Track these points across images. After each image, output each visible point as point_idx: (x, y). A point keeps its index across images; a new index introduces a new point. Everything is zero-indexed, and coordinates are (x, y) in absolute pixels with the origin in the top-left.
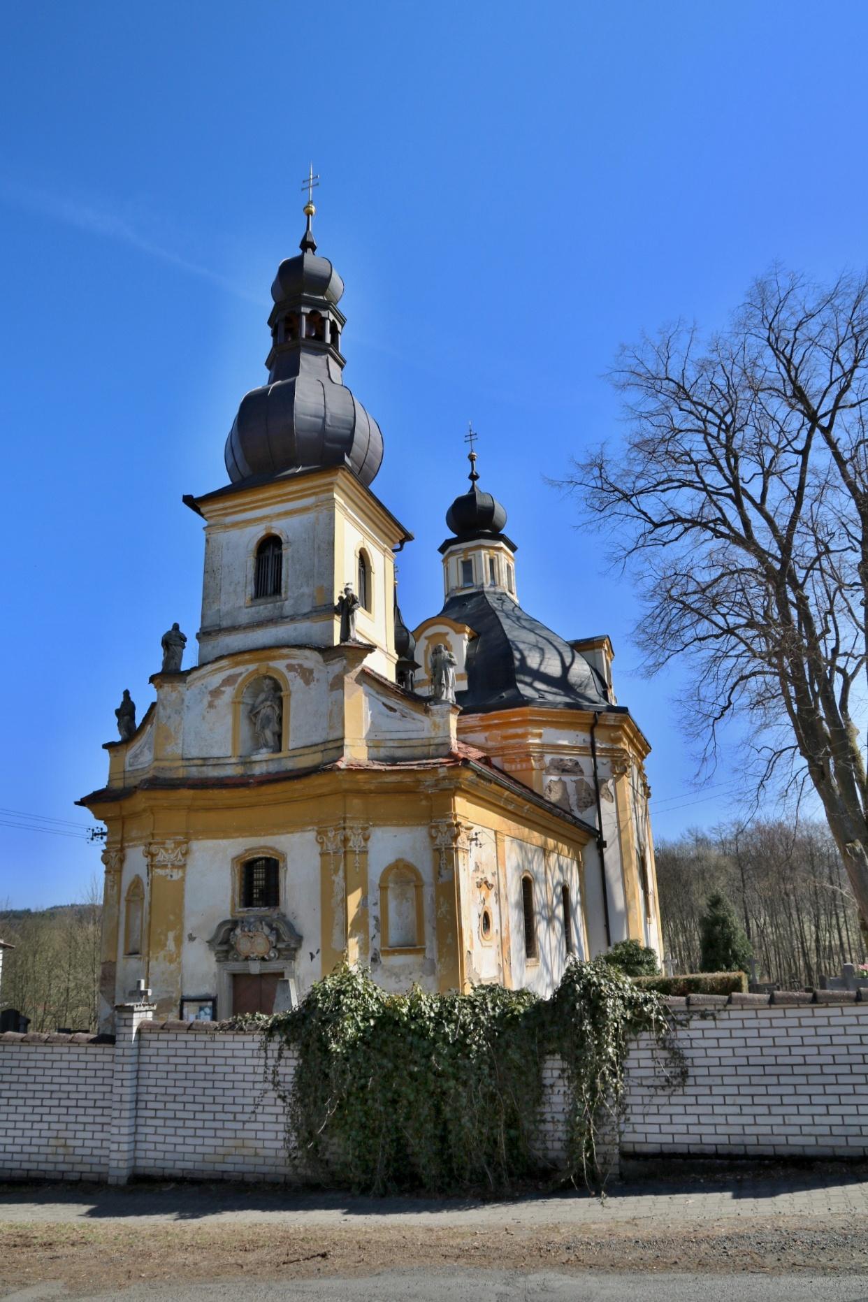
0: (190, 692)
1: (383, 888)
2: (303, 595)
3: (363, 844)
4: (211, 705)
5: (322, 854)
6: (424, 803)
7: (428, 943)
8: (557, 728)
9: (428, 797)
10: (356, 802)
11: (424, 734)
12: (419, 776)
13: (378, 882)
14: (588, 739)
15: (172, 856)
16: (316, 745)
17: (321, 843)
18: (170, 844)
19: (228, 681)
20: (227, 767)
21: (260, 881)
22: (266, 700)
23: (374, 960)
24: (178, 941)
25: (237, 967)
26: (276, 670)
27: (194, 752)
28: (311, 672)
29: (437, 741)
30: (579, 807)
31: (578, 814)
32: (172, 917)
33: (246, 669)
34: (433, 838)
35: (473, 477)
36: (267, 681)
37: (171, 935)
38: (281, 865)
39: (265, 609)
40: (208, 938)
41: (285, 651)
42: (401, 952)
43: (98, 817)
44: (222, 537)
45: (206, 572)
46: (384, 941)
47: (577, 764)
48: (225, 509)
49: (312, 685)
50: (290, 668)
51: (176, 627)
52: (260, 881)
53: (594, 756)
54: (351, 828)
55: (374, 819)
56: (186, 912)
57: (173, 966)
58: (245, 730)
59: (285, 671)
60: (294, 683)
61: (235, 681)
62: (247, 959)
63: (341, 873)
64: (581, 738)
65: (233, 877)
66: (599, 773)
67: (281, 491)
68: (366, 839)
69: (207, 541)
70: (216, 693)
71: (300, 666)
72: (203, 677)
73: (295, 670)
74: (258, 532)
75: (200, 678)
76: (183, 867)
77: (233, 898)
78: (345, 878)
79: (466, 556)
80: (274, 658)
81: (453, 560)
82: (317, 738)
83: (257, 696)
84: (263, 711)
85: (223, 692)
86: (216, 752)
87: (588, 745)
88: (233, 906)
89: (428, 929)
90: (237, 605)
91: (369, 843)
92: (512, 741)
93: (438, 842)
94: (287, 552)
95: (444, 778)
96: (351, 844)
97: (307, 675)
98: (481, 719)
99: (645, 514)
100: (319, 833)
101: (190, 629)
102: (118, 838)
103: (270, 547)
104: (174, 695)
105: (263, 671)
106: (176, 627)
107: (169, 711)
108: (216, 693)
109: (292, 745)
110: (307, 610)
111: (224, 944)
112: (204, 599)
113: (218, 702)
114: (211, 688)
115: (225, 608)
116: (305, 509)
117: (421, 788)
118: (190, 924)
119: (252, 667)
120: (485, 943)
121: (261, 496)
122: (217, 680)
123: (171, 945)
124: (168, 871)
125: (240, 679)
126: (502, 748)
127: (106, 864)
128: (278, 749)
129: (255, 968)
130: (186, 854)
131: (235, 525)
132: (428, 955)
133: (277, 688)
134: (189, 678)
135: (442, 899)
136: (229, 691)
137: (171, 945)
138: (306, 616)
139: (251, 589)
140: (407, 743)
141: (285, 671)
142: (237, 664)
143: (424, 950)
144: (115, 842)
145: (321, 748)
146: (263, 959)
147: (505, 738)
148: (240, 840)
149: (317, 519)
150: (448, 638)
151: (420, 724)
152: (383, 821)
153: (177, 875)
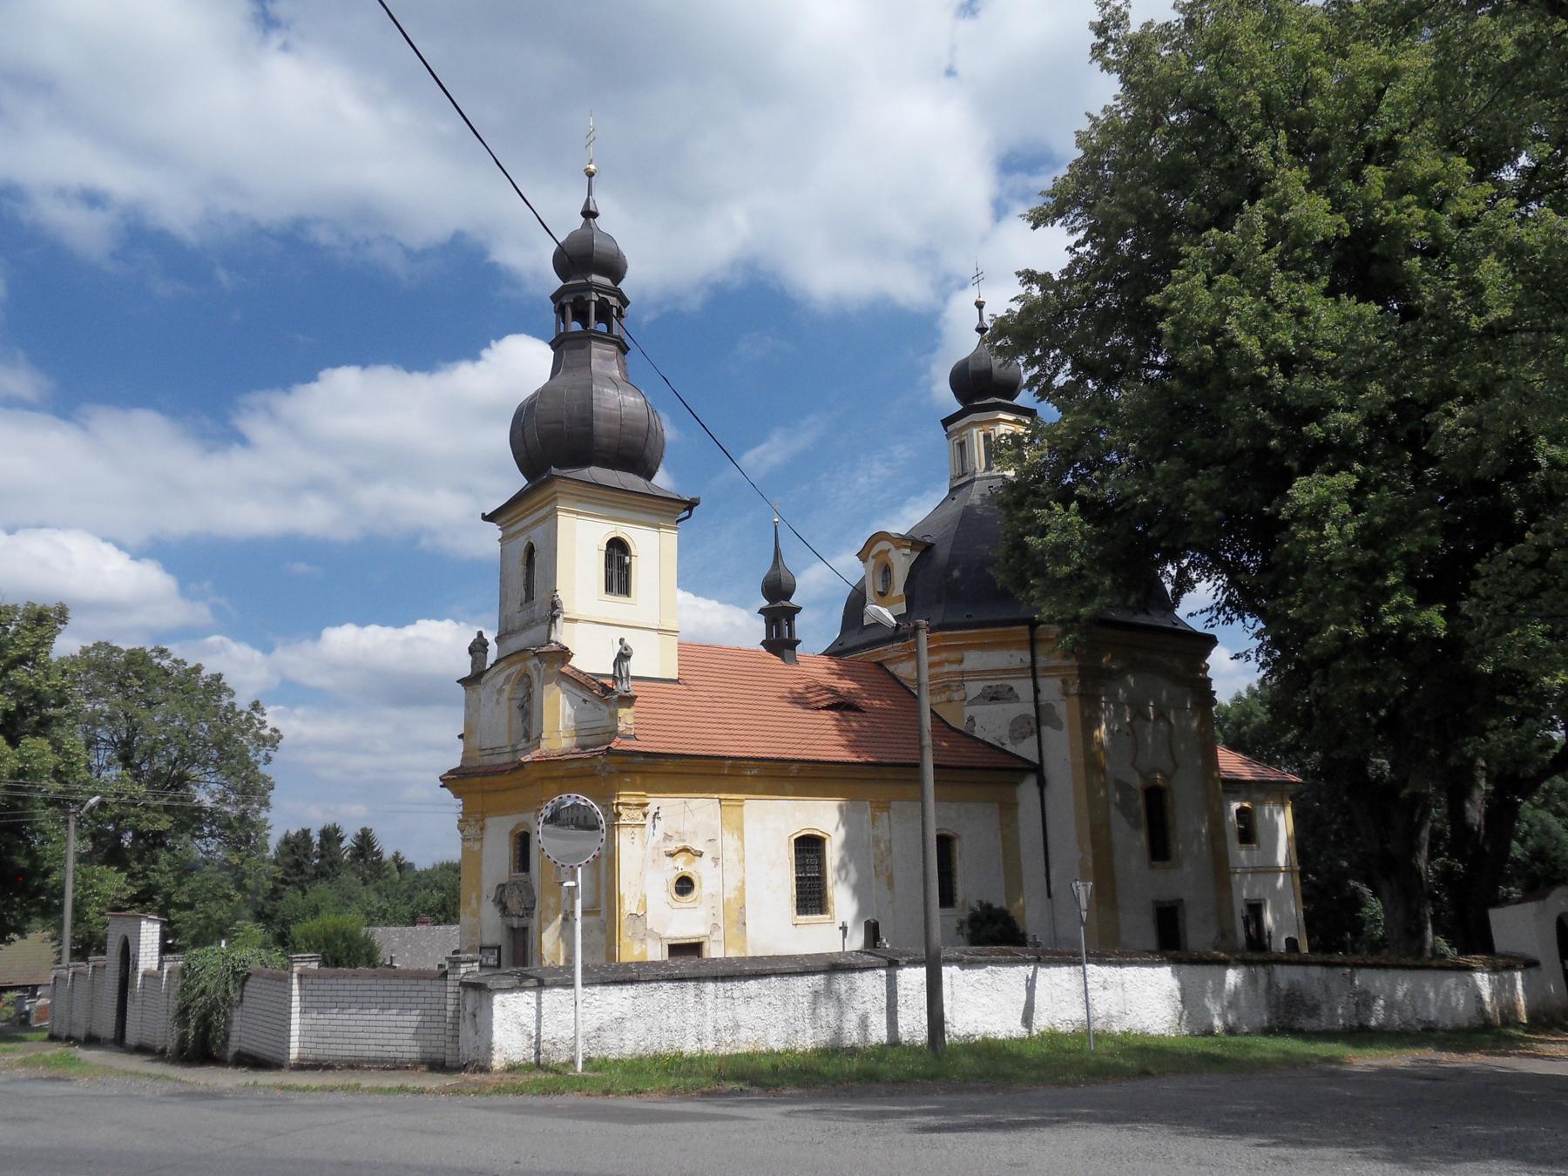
4: (498, 702)
11: (604, 723)
14: (1027, 657)
27: (487, 744)
31: (1009, 748)
47: (1011, 689)
53: (1034, 677)
64: (1020, 657)
101: (490, 636)
103: (530, 551)
108: (500, 691)
120: (676, 905)
136: (507, 688)
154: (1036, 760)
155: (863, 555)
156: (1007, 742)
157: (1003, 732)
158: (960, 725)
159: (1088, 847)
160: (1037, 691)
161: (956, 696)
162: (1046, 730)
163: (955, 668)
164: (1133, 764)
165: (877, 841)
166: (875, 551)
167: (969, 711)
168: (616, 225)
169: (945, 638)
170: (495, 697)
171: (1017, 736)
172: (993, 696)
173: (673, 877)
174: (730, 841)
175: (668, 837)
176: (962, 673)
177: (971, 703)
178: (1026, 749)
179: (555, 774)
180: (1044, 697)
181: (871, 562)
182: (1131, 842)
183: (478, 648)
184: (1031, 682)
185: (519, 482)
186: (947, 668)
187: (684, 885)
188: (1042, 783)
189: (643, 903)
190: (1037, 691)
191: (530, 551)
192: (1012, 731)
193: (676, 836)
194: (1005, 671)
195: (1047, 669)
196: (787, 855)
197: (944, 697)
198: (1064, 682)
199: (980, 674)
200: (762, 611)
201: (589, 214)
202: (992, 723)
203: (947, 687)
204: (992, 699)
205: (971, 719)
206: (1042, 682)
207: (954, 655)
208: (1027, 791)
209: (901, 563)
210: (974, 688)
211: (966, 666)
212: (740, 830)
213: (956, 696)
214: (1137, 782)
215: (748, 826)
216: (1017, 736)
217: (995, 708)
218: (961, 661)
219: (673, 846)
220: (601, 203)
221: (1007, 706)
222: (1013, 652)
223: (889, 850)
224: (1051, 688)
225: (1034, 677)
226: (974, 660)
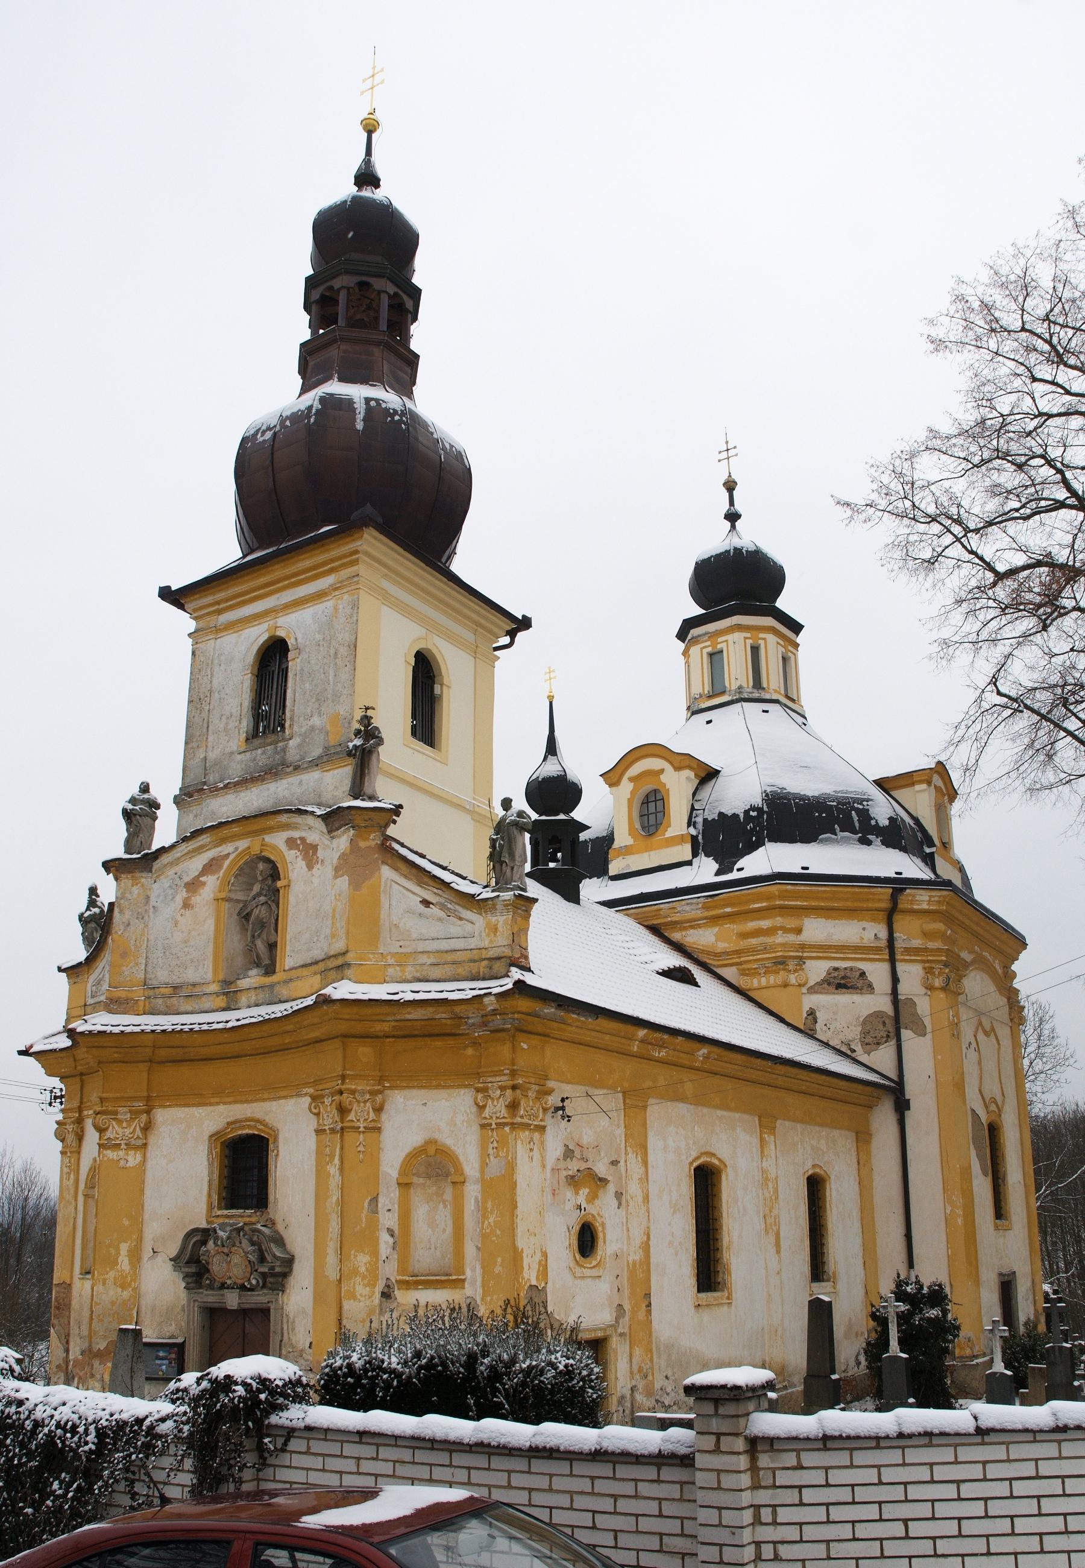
0: (160, 887)
1: (404, 1186)
2: (313, 729)
3: (372, 1116)
4: (186, 905)
5: (319, 1132)
6: (470, 1051)
7: (468, 1273)
8: (827, 917)
9: (475, 1043)
10: (364, 1052)
11: (473, 943)
12: (457, 1009)
13: (394, 1174)
14: (883, 934)
15: (127, 1131)
16: (316, 963)
17: (318, 1114)
18: (124, 1114)
19: (210, 867)
20: (204, 999)
21: (244, 1166)
22: (259, 894)
23: (386, 1295)
24: (135, 1256)
25: (210, 1297)
26: (274, 848)
27: (162, 975)
28: (315, 848)
29: (491, 954)
30: (865, 1044)
32: (126, 1223)
33: (234, 849)
34: (481, 1108)
35: (733, 517)
36: (261, 866)
37: (124, 1248)
38: (271, 1146)
39: (262, 756)
40: (173, 1252)
41: (284, 818)
42: (428, 1284)
43: (50, 1073)
44: (210, 645)
45: (190, 702)
46: (403, 1264)
48: (218, 603)
49: (315, 870)
50: (291, 843)
51: (145, 788)
52: (244, 1166)
53: (892, 961)
54: (353, 1092)
55: (387, 1079)
56: (146, 1216)
57: (126, 1294)
58: (235, 942)
59: (283, 847)
60: (294, 866)
61: (220, 867)
62: (223, 1286)
63: (337, 1161)
64: (871, 932)
65: (210, 1164)
66: (902, 988)
67: (288, 571)
68: (379, 1110)
69: (193, 653)
71: (303, 839)
72: (177, 861)
73: (297, 847)
74: (256, 636)
75: (172, 864)
76: (145, 1145)
77: (209, 1195)
78: (341, 1169)
79: (713, 645)
80: (270, 830)
81: (695, 650)
82: (318, 954)
83: (250, 886)
84: (256, 912)
85: (204, 884)
86: (191, 975)
87: (883, 943)
88: (210, 1208)
89: (470, 1250)
90: (228, 750)
92: (754, 941)
93: (487, 1113)
94: (295, 664)
95: (495, 1012)
96: (352, 1116)
97: (310, 852)
98: (706, 907)
99: (981, 559)
100: (314, 1098)
102: (75, 1104)
103: (273, 657)
104: (136, 890)
105: (256, 850)
106: (145, 788)
107: (128, 914)
108: (193, 886)
109: (289, 963)
110: (317, 752)
111: (194, 1260)
112: (186, 743)
113: (196, 900)
114: (186, 879)
115: (212, 755)
116: (320, 596)
117: (463, 1029)
118: (153, 1229)
119: (243, 844)
120: (579, 1271)
121: (263, 580)
122: (196, 865)
123: (124, 1263)
124: (121, 1153)
125: (227, 863)
126: (738, 952)
127: (62, 1141)
128: (270, 970)
129: (232, 1300)
130: (147, 1128)
131: (230, 626)
132: (468, 1291)
133: (274, 874)
134: (156, 865)
135: (489, 1205)
136: (211, 882)
137: (124, 1263)
138: (315, 764)
139: (246, 724)
140: (450, 957)
141: (283, 847)
142: (224, 841)
143: (463, 1281)
144: (71, 1110)
145: (321, 966)
146: (243, 1288)
147: (744, 935)
148: (221, 1107)
149: (336, 608)
150: (663, 778)
151: (468, 927)
153: (133, 1159)
154: (895, 1078)
156: (858, 1048)
160: (895, 980)
161: (793, 979)
162: (906, 1034)
163: (791, 938)
167: (810, 1001)
170: (183, 894)
171: (871, 1043)
176: (803, 947)
177: (812, 990)
179: (378, 1028)
180: (905, 989)
181: (626, 787)
183: (139, 814)
184: (885, 967)
185: (226, 550)
186: (780, 938)
190: (895, 980)
191: (273, 657)
192: (865, 1033)
194: (856, 949)
195: (908, 951)
198: (929, 971)
199: (824, 950)
203: (781, 963)
205: (812, 1013)
206: (901, 967)
207: (790, 923)
210: (817, 969)
213: (793, 979)
215: (654, 1143)
217: (843, 999)
218: (799, 931)
221: (857, 998)
222: (865, 924)
224: (911, 976)
225: (892, 961)
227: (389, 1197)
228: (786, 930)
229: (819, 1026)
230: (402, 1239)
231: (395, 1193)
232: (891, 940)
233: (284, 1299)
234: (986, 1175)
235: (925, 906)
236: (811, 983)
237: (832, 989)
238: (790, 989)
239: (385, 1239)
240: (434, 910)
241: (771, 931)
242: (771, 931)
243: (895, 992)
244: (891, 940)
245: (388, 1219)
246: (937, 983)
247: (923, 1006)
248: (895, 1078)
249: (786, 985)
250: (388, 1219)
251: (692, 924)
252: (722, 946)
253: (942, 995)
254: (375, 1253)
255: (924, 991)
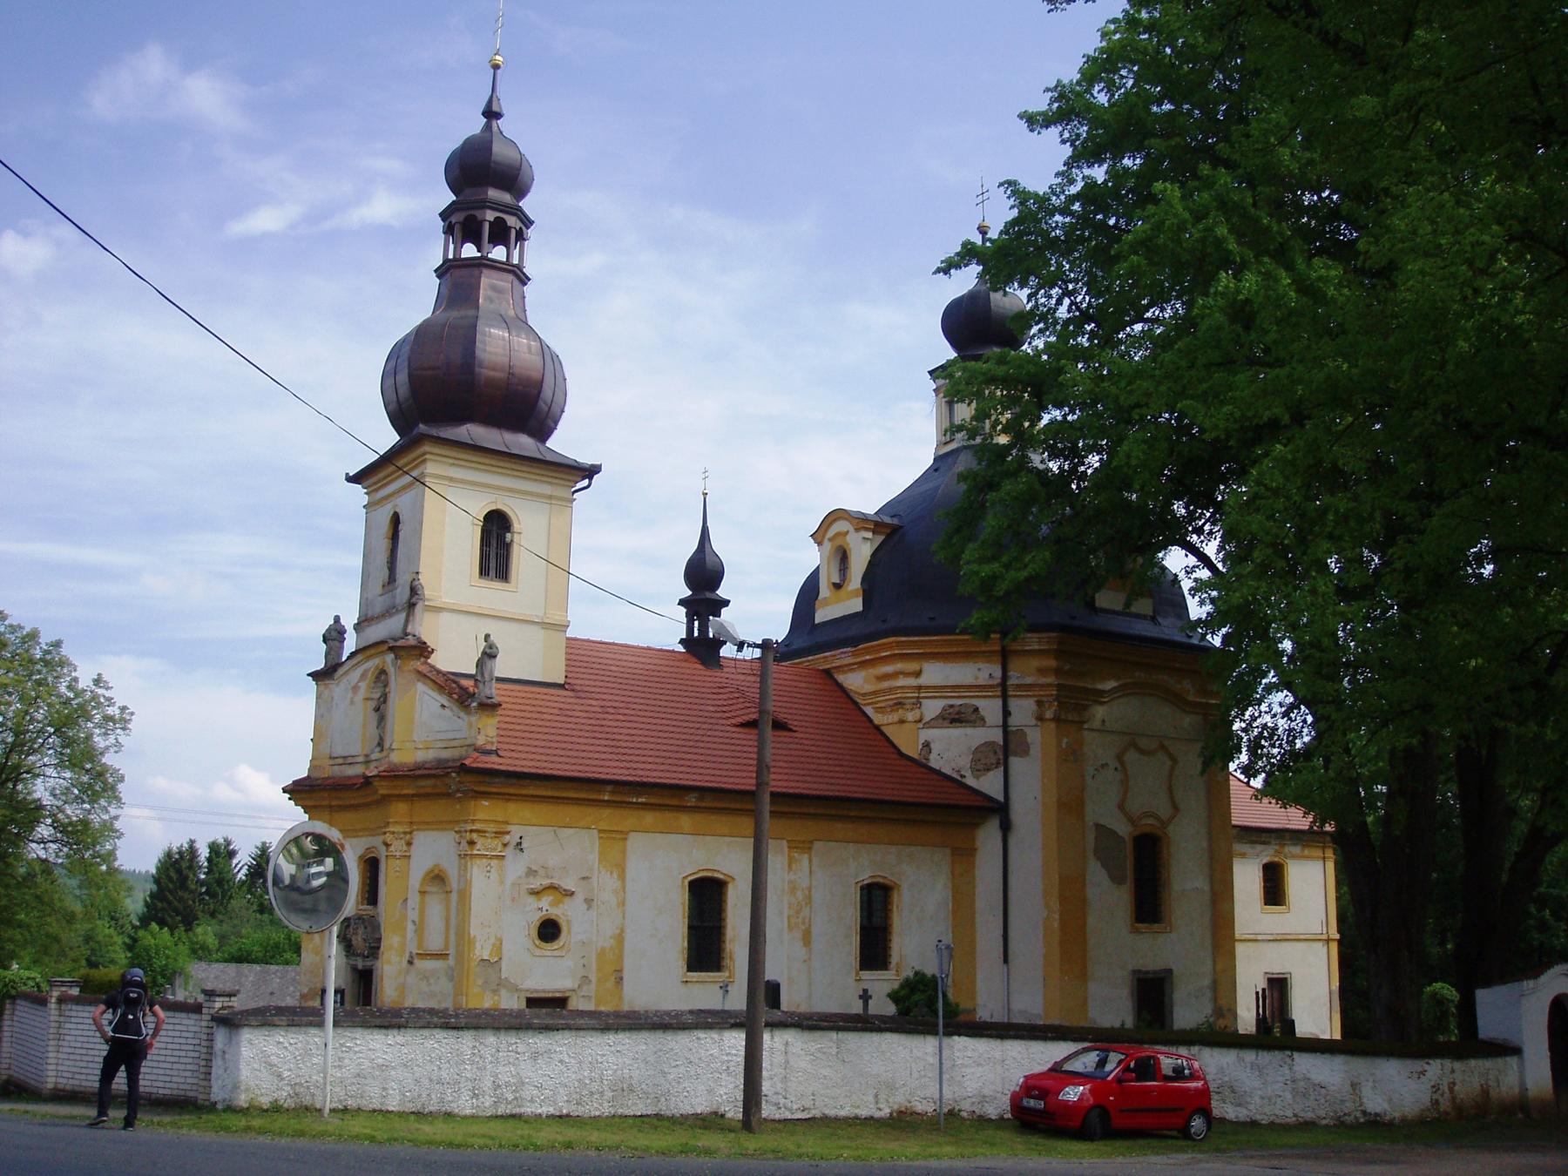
4: (352, 702)
14: (998, 673)
19: (363, 676)
23: (410, 963)
27: (339, 751)
31: (970, 781)
46: (420, 946)
47: (976, 710)
51: (337, 619)
66: (1012, 721)
70: (355, 688)
91: (413, 848)
98: (854, 654)
101: (349, 621)
103: (396, 520)
106: (337, 619)
108: (355, 688)
120: (538, 952)
126: (874, 693)
134: (337, 675)
136: (363, 685)
147: (881, 678)
152: (428, 825)
154: (1001, 799)
155: (818, 537)
156: (968, 774)
157: (964, 762)
158: (912, 751)
159: (1055, 905)
160: (1006, 713)
161: (910, 716)
162: (1015, 762)
163: (912, 682)
164: (1121, 807)
165: (793, 890)
166: (831, 533)
168: (523, 133)
169: (899, 645)
170: (350, 695)
171: (980, 768)
172: (954, 718)
173: (535, 919)
174: (606, 883)
175: (531, 873)
176: (919, 688)
177: (929, 725)
178: (990, 784)
180: (1015, 720)
181: (827, 545)
182: (1109, 899)
183: (334, 636)
184: (999, 702)
185: (388, 437)
186: (901, 682)
187: (549, 931)
188: (1006, 827)
189: (498, 947)
190: (1006, 713)
191: (396, 520)
193: (542, 872)
195: (1019, 687)
196: (679, 901)
197: (895, 717)
198: (1039, 703)
199: (939, 690)
200: (682, 602)
201: (491, 114)
202: (950, 750)
203: (899, 704)
204: (953, 721)
205: (927, 745)
206: (1013, 704)
207: (912, 666)
208: (988, 837)
209: (862, 551)
210: (932, 708)
211: (924, 680)
212: (621, 869)
214: (1123, 829)
215: (634, 865)
216: (980, 768)
217: (956, 733)
218: (918, 674)
219: (537, 883)
220: (505, 105)
221: (969, 731)
222: (981, 665)
223: (809, 899)
224: (1023, 710)
225: (1005, 697)
226: (935, 673)
227: (414, 900)
228: (907, 674)
229: (932, 757)
230: (420, 927)
231: (417, 898)
232: (1005, 677)
233: (378, 964)
234: (1117, 879)
235: (1036, 647)
236: (927, 719)
237: (946, 723)
238: (907, 725)
239: (410, 927)
240: (447, 711)
241: (895, 675)
242: (895, 675)
243: (1005, 726)
244: (1005, 677)
245: (413, 915)
246: (1049, 714)
247: (1034, 736)
248: (1001, 799)
249: (902, 722)
250: (413, 915)
251: (848, 668)
252: (869, 688)
253: (1053, 725)
254: (404, 937)
255: (1034, 722)
